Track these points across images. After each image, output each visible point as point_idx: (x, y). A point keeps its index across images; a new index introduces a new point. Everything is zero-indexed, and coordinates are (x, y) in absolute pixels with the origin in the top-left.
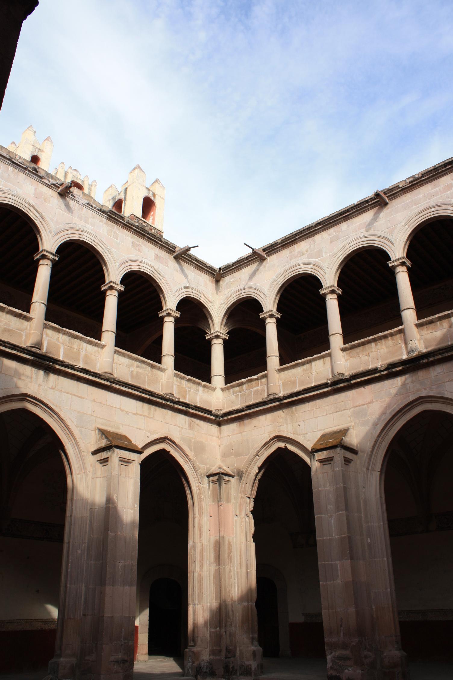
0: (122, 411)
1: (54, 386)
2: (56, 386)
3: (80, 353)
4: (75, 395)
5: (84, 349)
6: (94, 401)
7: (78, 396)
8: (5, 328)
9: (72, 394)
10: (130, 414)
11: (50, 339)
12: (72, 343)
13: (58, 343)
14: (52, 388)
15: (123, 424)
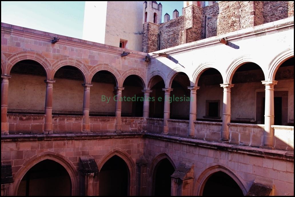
0: (274, 170)
1: (231, 159)
2: (232, 159)
3: (250, 135)
4: (243, 163)
5: (252, 132)
6: (254, 165)
7: (245, 164)
8: (212, 133)
9: (241, 163)
10: (280, 172)
11: (233, 131)
12: (245, 130)
13: (237, 133)
14: (230, 161)
15: (275, 179)
